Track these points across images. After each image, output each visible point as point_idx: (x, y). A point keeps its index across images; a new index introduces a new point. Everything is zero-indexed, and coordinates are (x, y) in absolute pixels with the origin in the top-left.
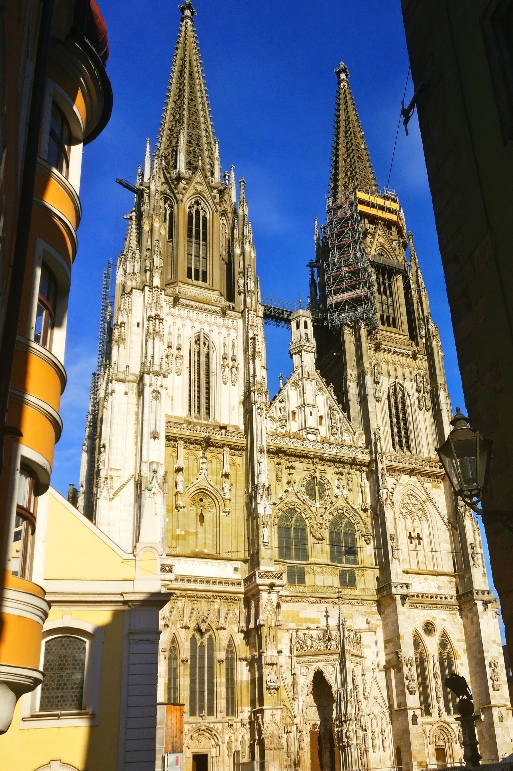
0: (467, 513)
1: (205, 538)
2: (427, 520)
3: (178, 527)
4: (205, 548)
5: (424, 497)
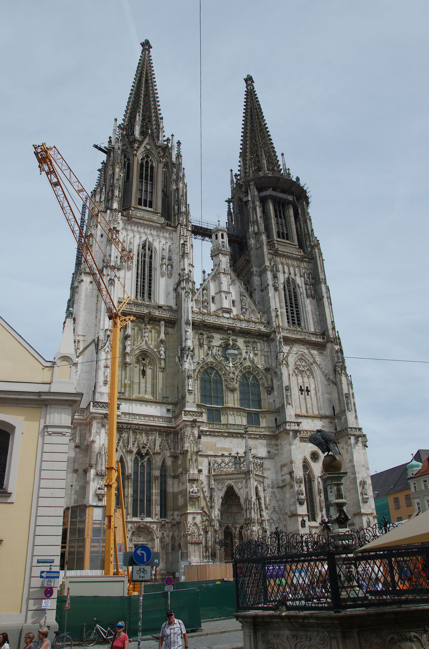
0: (343, 372)
1: (146, 387)
2: (313, 378)
3: (125, 378)
4: (146, 395)
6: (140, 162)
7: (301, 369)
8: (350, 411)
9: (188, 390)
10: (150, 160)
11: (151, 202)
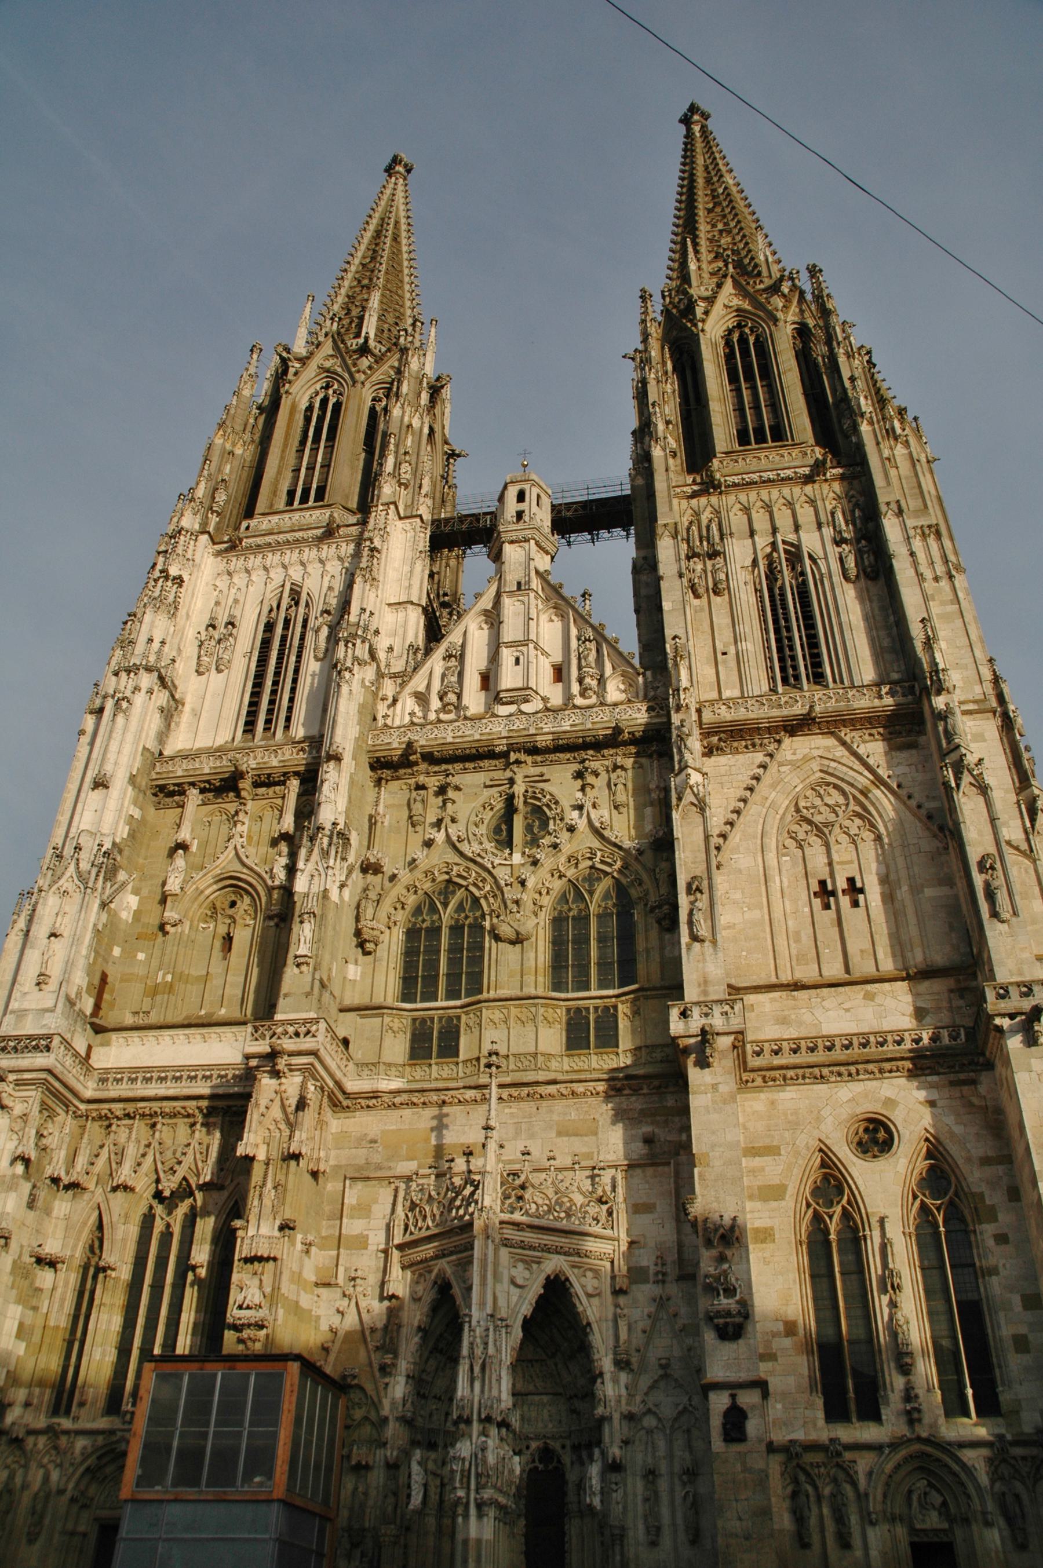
0: (966, 778)
3: (160, 969)
5: (864, 780)
6: (304, 404)
7: (818, 819)
9: (296, 957)
10: (335, 392)
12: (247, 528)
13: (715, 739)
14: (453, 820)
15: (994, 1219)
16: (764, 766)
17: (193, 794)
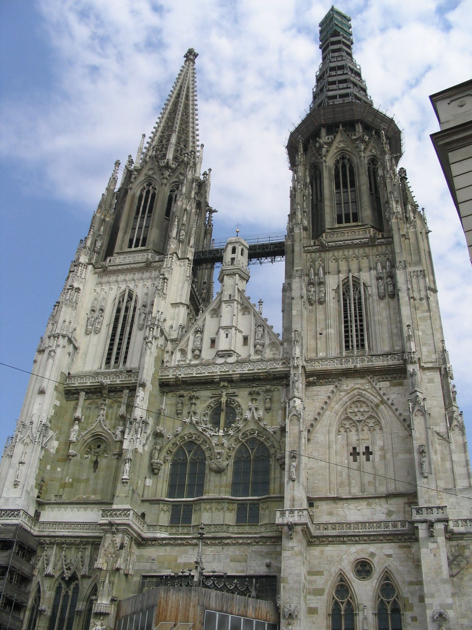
2: (381, 429)
8: (426, 477)
9: (123, 479)
10: (153, 188)
11: (145, 239)
12: (110, 261)
13: (311, 379)
14: (195, 413)
15: (411, 609)
16: (333, 392)
17: (83, 394)
